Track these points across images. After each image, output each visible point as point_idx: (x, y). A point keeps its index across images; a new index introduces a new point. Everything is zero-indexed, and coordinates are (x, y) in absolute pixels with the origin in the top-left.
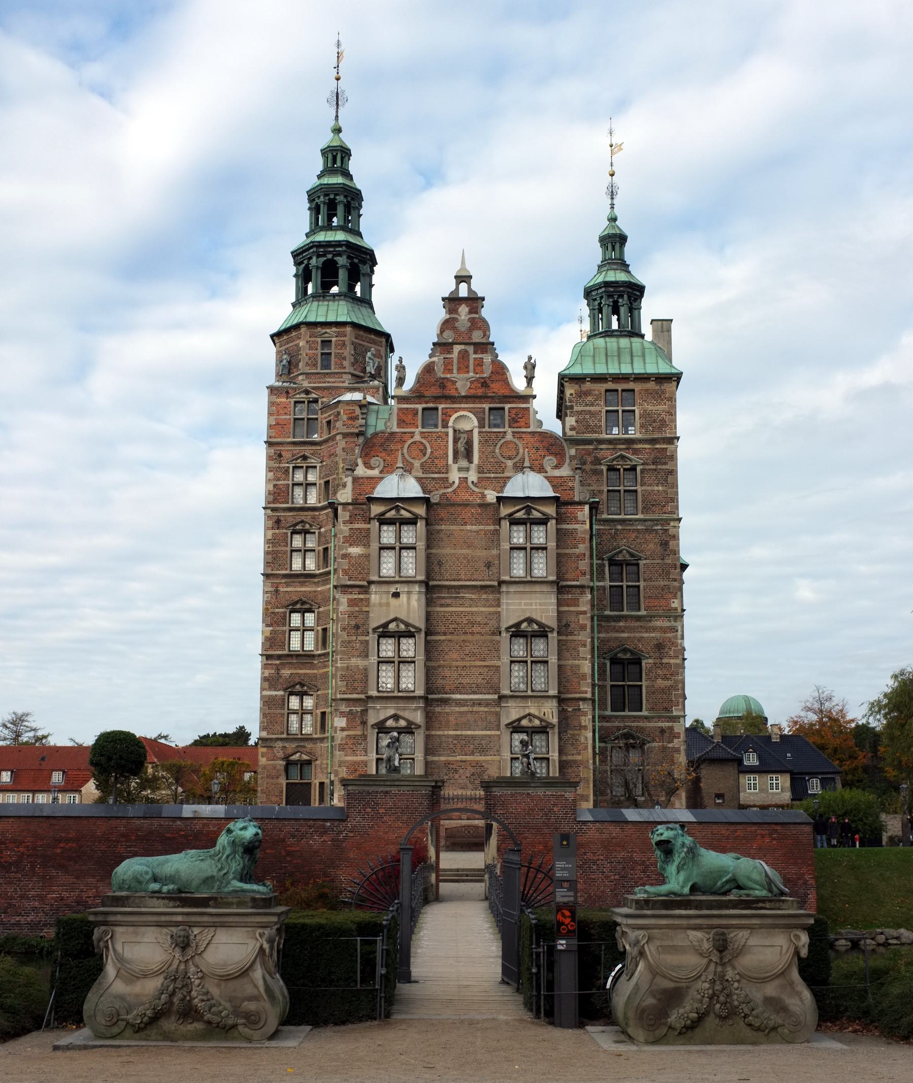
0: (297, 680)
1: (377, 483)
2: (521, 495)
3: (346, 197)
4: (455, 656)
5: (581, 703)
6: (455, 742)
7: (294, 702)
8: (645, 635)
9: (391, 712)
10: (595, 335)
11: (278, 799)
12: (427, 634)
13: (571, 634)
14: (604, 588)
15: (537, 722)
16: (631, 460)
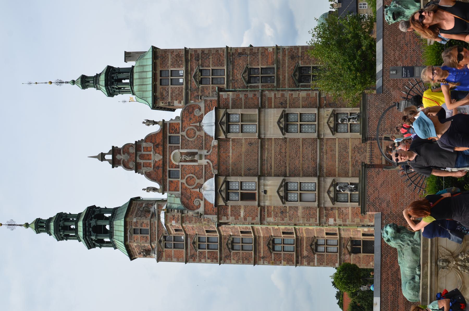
0: (309, 247)
1: (208, 202)
2: (214, 128)
3: (60, 221)
4: (297, 162)
5: (322, 96)
6: (342, 162)
7: (321, 249)
8: (287, 65)
9: (326, 195)
10: (132, 91)
11: (371, 258)
12: (286, 176)
13: (286, 101)
15: (332, 119)
16: (196, 72)
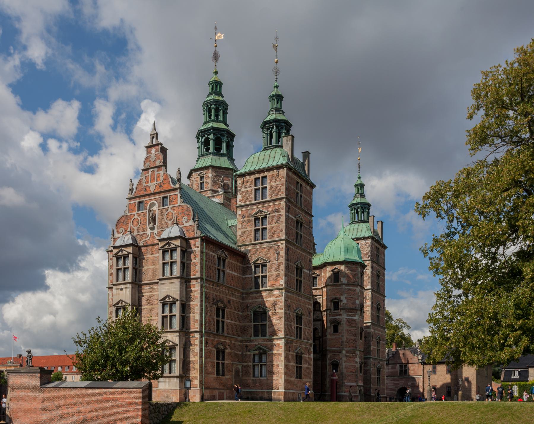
14: (252, 278)
